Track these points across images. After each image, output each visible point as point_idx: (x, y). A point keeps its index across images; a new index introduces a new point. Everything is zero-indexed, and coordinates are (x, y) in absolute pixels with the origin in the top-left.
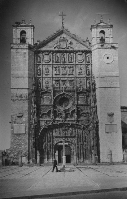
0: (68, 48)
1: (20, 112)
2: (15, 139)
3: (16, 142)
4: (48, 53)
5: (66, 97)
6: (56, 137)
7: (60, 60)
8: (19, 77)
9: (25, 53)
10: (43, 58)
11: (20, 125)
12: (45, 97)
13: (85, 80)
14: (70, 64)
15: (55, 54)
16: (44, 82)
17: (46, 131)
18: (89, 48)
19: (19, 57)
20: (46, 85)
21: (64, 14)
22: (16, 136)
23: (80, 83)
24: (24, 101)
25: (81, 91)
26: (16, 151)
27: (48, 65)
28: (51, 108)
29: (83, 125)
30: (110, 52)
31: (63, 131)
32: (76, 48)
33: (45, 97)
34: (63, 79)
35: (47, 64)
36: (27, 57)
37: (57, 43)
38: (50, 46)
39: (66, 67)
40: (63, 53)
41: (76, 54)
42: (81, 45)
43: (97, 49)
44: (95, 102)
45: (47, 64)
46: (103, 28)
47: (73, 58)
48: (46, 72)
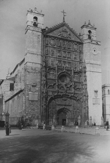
0: (68, 38)
1: (34, 83)
3: (31, 107)
4: (53, 39)
7: (62, 46)
8: (34, 54)
9: (39, 35)
11: (34, 93)
14: (69, 50)
16: (50, 60)
17: (52, 99)
20: (52, 63)
21: (64, 12)
22: (31, 102)
23: (75, 65)
24: (37, 74)
26: (31, 114)
27: (54, 47)
28: (56, 81)
30: (96, 47)
31: (63, 101)
33: (51, 72)
36: (41, 39)
37: (60, 32)
39: (66, 52)
40: (64, 41)
42: (76, 38)
45: (53, 47)
46: (91, 29)
48: (52, 53)
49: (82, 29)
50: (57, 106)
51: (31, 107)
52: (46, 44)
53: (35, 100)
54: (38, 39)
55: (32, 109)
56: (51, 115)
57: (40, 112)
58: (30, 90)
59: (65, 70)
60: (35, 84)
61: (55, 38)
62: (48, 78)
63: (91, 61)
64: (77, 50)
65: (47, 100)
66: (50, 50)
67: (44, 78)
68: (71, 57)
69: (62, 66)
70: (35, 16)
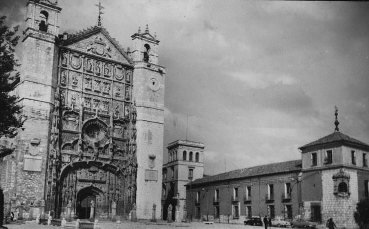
0: (105, 56)
2: (25, 179)
3: (26, 183)
4: (78, 55)
5: (99, 124)
6: (81, 181)
8: (37, 83)
9: (49, 49)
10: (70, 60)
11: (34, 157)
12: (70, 119)
13: (124, 106)
14: (106, 79)
15: (87, 58)
18: (131, 64)
19: (40, 51)
20: (72, 103)
23: (117, 108)
24: (43, 121)
25: (118, 119)
26: (26, 198)
27: (77, 72)
28: (79, 136)
29: (118, 166)
30: (156, 77)
31: (91, 174)
32: (115, 58)
33: (70, 119)
34: (96, 98)
35: (76, 72)
36: (53, 55)
37: (91, 44)
38: (83, 46)
39: (100, 82)
40: (98, 61)
41: (114, 66)
42: (121, 56)
43: (143, 69)
44: (134, 137)
46: (149, 42)
47: (110, 72)
48: (74, 83)
49: (133, 39)
50: (78, 183)
51: (26, 183)
52: (63, 65)
53: (35, 170)
54: (48, 56)
55: (28, 188)
56: (66, 199)
57: (45, 193)
58: (27, 151)
59: (96, 117)
60: (37, 141)
61: (81, 54)
62: (64, 128)
63: (146, 101)
64: (122, 79)
65: (60, 172)
66: (71, 78)
67: (55, 130)
68: (110, 93)
69: (91, 108)
70: (43, 9)
